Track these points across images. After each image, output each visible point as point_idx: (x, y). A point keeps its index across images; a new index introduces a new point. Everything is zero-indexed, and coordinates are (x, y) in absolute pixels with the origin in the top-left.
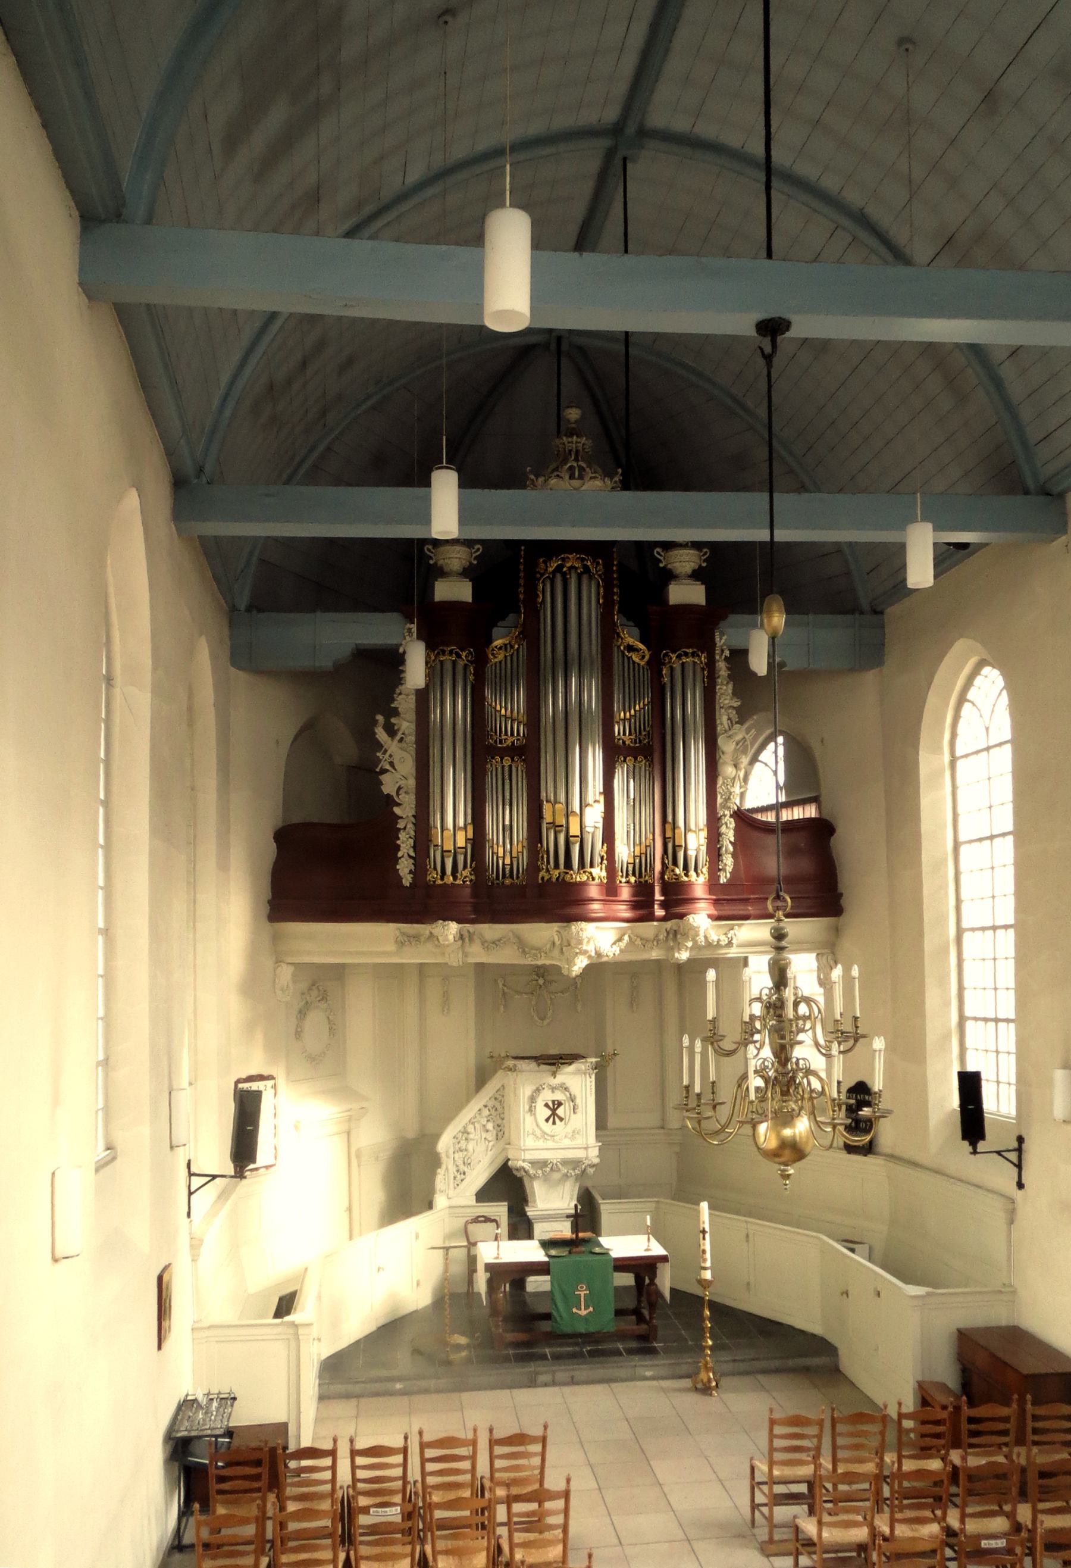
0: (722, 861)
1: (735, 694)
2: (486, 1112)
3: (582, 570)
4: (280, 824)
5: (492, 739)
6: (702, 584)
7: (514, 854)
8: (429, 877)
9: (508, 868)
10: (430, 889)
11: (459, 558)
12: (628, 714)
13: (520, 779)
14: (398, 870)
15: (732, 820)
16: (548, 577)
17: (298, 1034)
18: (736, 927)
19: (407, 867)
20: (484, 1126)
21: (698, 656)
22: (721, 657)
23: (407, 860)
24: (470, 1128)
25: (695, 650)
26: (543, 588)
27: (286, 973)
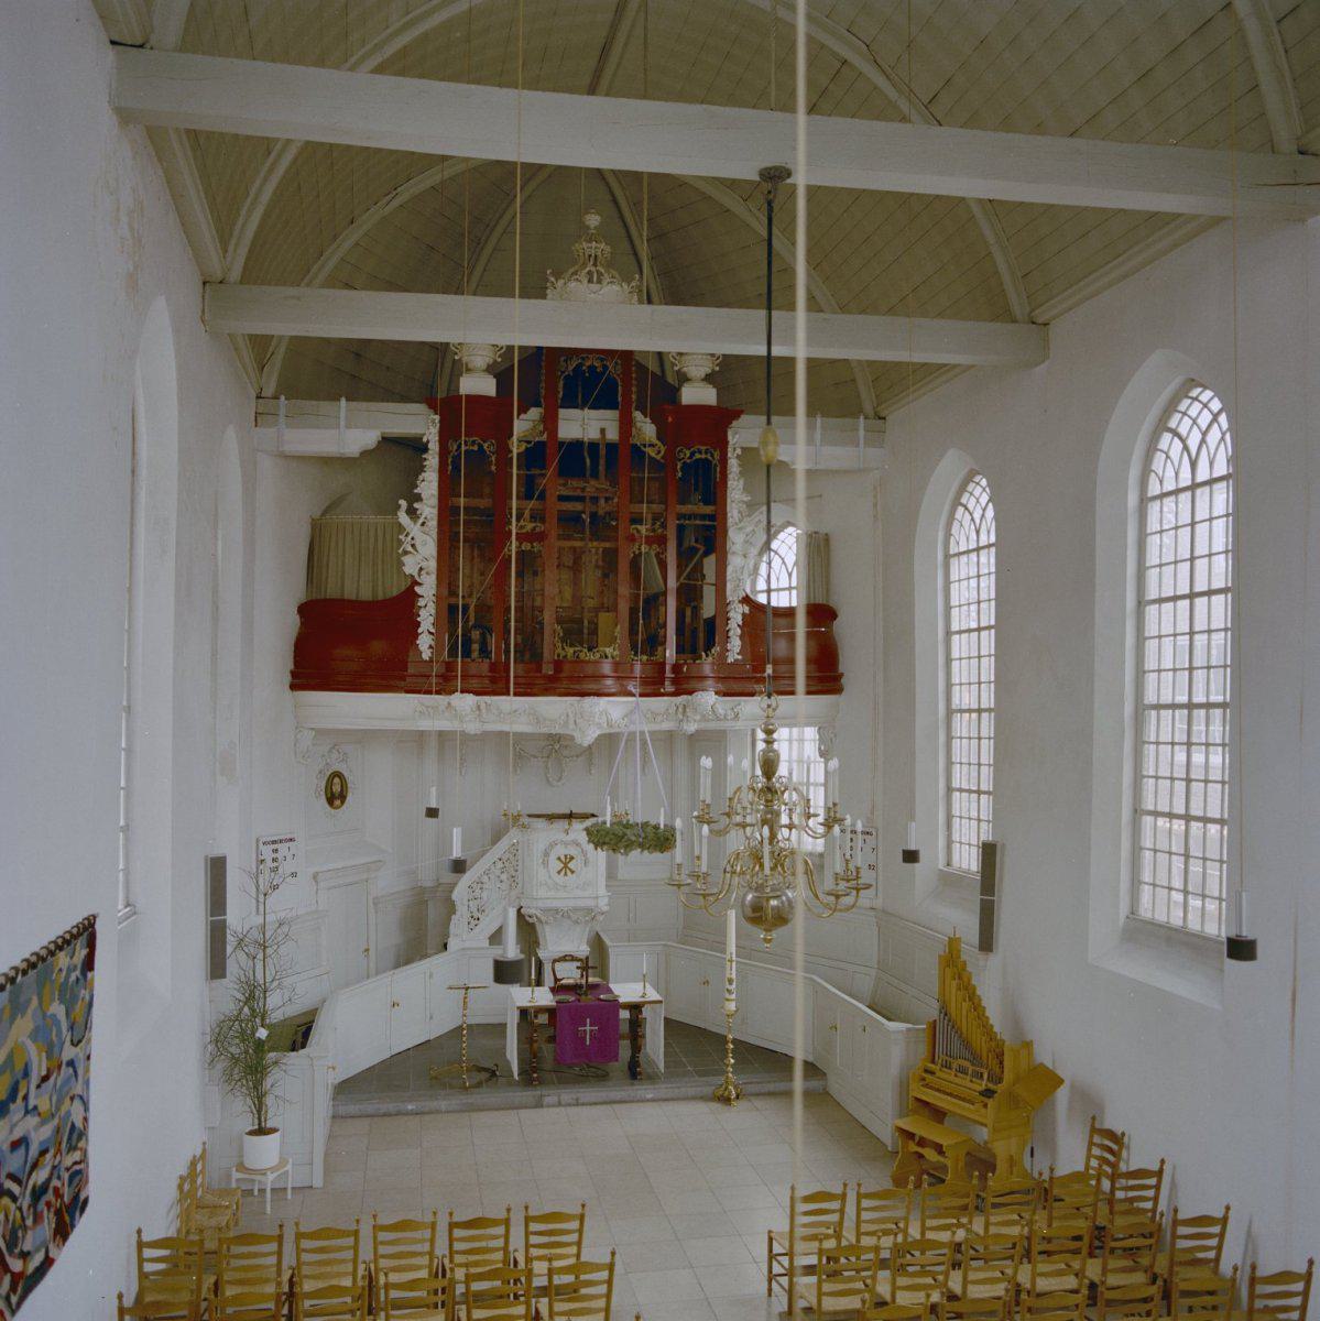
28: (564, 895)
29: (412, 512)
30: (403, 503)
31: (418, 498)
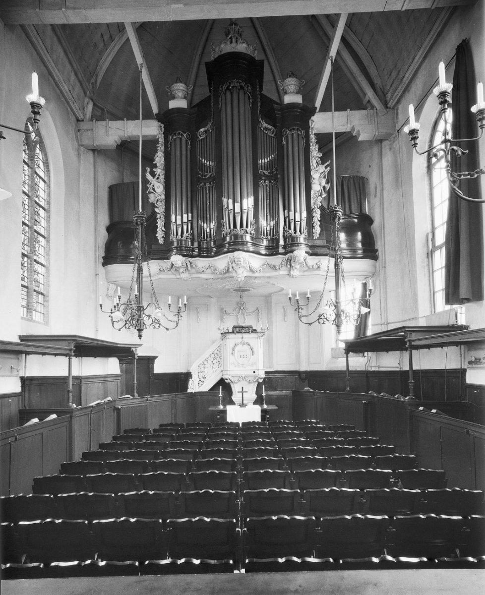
21: (300, 131)
24: (206, 362)
29: (153, 174)
30: (148, 169)
31: (155, 166)
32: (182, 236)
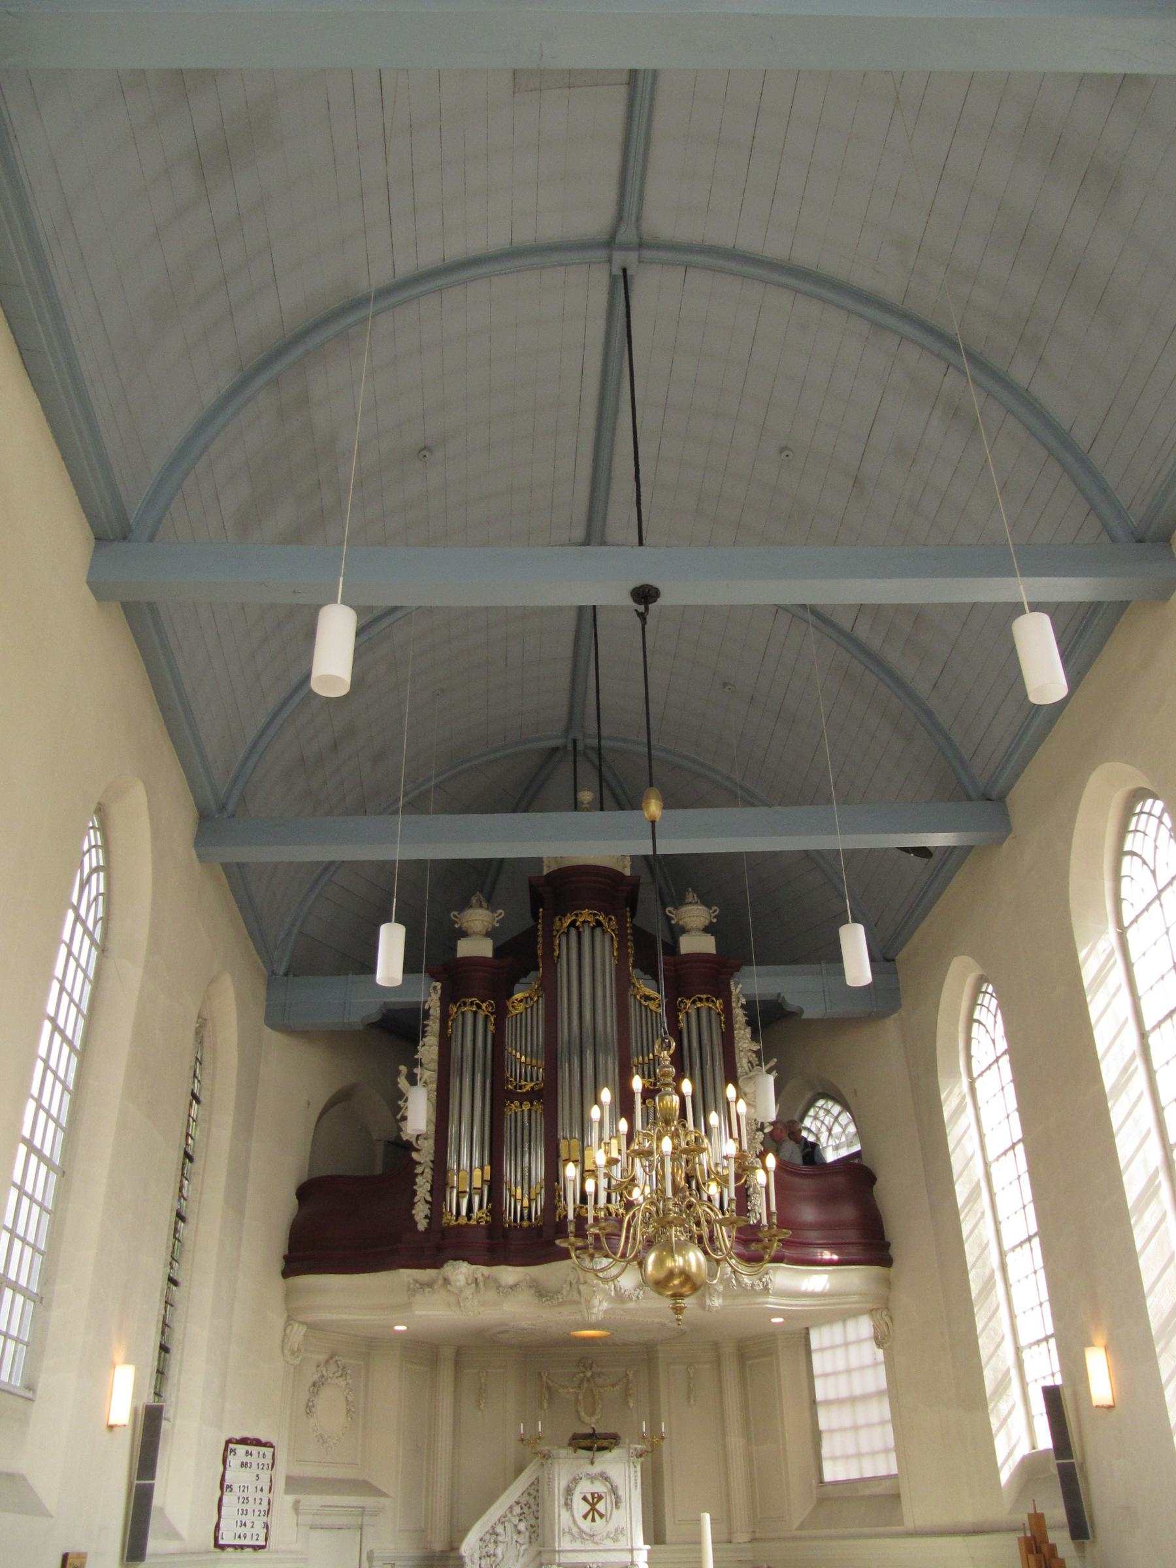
0: (751, 1202)
1: (754, 1037)
2: (517, 1510)
3: (594, 924)
4: (305, 1179)
5: (511, 1085)
6: (712, 935)
7: (533, 1197)
8: (444, 1221)
9: (526, 1211)
10: (446, 1231)
11: (482, 921)
12: (646, 1059)
13: (539, 1124)
14: (414, 1215)
15: (758, 1159)
16: (564, 932)
17: (309, 1409)
18: (771, 1271)
19: (423, 1211)
20: (516, 1526)
21: (713, 1001)
22: (737, 1005)
23: (423, 1205)
24: (500, 1529)
25: (709, 996)
26: (559, 944)
27: (298, 1332)
28: (591, 1546)
32: (469, 1217)
